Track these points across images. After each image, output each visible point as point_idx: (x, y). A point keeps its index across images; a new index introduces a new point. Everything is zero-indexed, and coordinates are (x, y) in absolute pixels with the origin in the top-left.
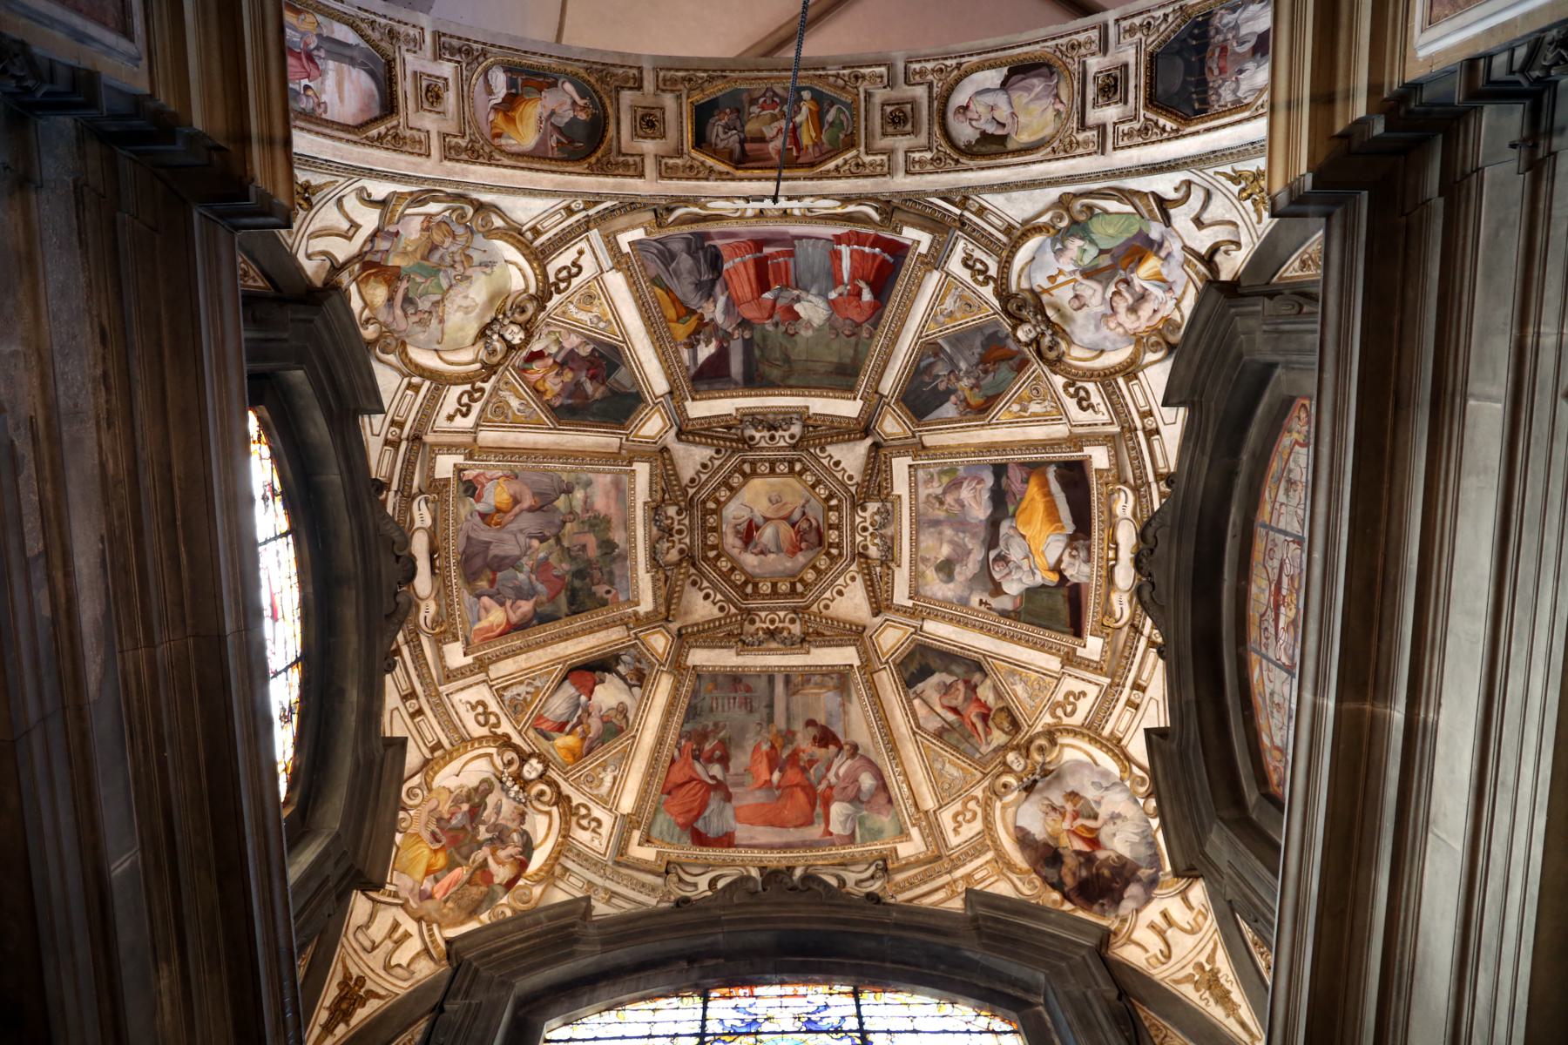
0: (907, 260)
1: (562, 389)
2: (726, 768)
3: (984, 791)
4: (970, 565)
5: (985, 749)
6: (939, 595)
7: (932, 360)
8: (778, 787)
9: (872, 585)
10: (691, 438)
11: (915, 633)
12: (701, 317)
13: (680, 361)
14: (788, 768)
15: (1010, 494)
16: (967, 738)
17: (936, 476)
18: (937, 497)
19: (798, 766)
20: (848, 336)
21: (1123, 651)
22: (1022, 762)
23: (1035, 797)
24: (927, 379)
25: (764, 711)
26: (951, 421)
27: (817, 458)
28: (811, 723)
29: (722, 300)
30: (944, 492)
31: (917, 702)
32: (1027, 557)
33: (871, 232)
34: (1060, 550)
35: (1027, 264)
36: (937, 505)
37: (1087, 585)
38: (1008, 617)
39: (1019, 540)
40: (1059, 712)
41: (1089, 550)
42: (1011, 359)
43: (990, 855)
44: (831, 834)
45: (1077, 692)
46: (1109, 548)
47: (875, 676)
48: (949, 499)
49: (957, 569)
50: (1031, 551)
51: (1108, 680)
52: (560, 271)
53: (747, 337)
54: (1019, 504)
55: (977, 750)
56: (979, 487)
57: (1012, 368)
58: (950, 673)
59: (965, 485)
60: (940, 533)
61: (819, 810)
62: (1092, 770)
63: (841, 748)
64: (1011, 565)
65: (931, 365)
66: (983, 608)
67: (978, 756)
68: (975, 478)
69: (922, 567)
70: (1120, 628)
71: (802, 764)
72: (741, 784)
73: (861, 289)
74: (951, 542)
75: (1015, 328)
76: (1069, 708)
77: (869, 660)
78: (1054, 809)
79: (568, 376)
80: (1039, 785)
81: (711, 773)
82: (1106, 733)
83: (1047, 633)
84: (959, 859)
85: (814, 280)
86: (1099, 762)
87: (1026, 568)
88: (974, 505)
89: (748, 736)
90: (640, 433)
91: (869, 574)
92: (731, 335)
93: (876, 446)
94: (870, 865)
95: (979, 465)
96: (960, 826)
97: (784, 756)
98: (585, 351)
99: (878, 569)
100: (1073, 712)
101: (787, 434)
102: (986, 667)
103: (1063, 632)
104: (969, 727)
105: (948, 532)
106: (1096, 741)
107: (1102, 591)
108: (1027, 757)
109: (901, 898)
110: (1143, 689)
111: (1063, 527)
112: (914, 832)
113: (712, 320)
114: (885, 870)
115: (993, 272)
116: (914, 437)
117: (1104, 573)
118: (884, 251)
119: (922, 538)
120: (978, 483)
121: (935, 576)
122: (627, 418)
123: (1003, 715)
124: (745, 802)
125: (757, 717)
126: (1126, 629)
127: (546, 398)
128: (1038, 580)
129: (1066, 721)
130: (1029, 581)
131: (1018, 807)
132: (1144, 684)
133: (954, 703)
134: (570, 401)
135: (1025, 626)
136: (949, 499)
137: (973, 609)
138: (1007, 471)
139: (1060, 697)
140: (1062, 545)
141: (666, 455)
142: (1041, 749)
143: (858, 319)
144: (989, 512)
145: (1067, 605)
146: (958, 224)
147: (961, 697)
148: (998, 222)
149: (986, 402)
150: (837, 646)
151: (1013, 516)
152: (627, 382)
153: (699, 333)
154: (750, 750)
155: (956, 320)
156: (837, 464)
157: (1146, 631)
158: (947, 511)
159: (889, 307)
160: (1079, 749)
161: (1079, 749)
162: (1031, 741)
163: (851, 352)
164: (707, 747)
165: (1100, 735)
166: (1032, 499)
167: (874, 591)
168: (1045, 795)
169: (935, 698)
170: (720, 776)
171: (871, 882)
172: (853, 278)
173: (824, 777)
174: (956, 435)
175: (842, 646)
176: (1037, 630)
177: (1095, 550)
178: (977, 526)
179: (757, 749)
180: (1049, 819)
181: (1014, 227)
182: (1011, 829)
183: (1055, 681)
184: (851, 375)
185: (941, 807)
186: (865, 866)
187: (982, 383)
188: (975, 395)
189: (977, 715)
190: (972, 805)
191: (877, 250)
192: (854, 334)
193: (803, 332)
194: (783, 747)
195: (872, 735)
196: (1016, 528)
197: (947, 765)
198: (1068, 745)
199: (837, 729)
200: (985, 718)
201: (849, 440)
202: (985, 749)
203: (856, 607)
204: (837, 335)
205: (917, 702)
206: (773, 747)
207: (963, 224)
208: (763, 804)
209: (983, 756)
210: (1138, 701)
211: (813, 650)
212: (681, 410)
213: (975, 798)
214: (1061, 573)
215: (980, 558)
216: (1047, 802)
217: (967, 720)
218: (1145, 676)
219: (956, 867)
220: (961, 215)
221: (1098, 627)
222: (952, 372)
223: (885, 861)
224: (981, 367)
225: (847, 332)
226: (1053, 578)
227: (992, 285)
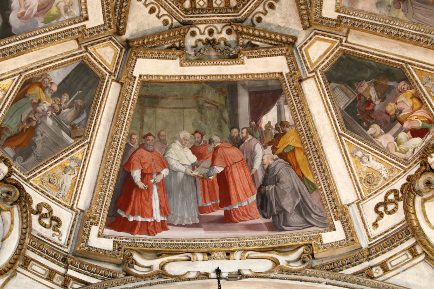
0: (106, 214)
1: (397, 96)
7: (77, 122)
10: (284, 39)
12: (274, 150)
13: (293, 110)
17: (63, 11)
20: (150, 134)
24: (79, 102)
26: (54, 67)
27: (171, 15)
29: (257, 166)
33: (137, 236)
35: (8, 236)
42: (9, 138)
52: (394, 211)
53: (235, 130)
56: (22, 10)
57: (7, 129)
59: (35, 10)
65: (77, 116)
68: (27, 18)
73: (142, 180)
75: (11, 172)
79: (391, 108)
85: (181, 185)
90: (329, 44)
92: (249, 132)
93: (119, 33)
95: (25, 31)
98: (375, 129)
101: (198, 36)
113: (265, 147)
115: (35, 218)
116: (86, 47)
118: (126, 219)
120: (23, 14)
122: (341, 59)
127: (413, 91)
134: (391, 84)
141: (307, 23)
143: (142, 152)
146: (69, 260)
148: (36, 268)
149: (26, 92)
152: (339, 94)
153: (276, 135)
155: (60, 165)
156: (152, 11)
159: (118, 167)
163: (146, 119)
172: (149, 190)
174: (49, 55)
181: (23, 266)
184: (145, 96)
187: (31, 108)
188: (36, 96)
191: (131, 219)
192: (145, 137)
193: (188, 135)
201: (143, 38)
204: (159, 135)
207: (64, 260)
212: (292, 63)
220: (67, 268)
222: (58, 114)
224: (34, 124)
225: (151, 138)
227: (34, 207)
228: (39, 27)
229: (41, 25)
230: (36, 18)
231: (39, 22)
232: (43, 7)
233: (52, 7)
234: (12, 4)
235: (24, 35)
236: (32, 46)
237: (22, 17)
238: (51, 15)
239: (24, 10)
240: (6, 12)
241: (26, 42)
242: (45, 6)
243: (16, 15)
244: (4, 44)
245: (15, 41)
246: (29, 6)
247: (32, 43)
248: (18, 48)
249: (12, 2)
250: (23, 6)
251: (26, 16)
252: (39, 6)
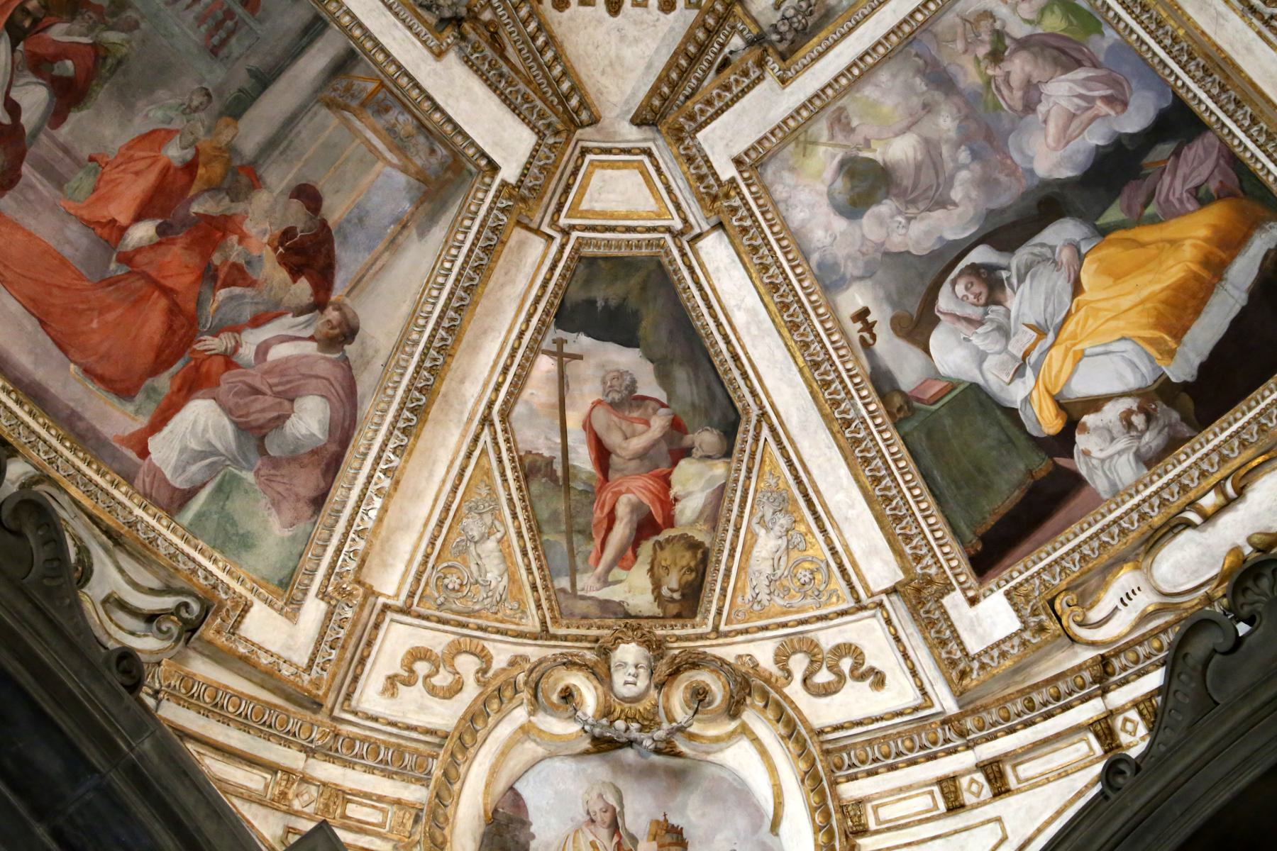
2: (56, 116)
3: (513, 663)
4: (917, 228)
5: (587, 583)
6: (797, 216)
8: (126, 259)
9: (693, 60)
11: (676, 235)
14: (182, 240)
15: (1146, 186)
16: (576, 530)
18: (999, 35)
19: (206, 256)
21: (1036, 687)
22: (642, 683)
23: (597, 769)
25: (242, 79)
28: (308, 196)
30: (1024, 44)
31: (545, 364)
32: (1041, 331)
34: (1118, 388)
36: (982, 51)
37: (1098, 501)
38: (883, 397)
39: (1062, 284)
40: (798, 664)
41: (1172, 445)
43: (415, 794)
44: (144, 453)
45: (870, 662)
46: (1219, 487)
47: (518, 234)
48: (1019, 66)
49: (885, 208)
50: (1059, 329)
51: (952, 707)
54: (1142, 221)
55: (573, 572)
56: (1102, 107)
58: (664, 377)
59: (1080, 74)
60: (928, 108)
61: (164, 383)
62: (756, 828)
63: (319, 304)
64: (995, 312)
66: (854, 329)
67: (564, 583)
68: (1112, 82)
69: (821, 128)
70: (1073, 640)
71: (216, 259)
72: (59, 181)
74: (930, 146)
76: (824, 676)
77: (537, 191)
78: (614, 827)
80: (629, 755)
81: (14, 95)
82: (850, 791)
83: (928, 502)
84: (352, 740)
86: (784, 828)
87: (1017, 346)
88: (1052, 128)
89: (161, 94)
91: (710, 33)
94: (167, 591)
95: (1151, 72)
96: (408, 683)
97: (196, 208)
99: (736, 42)
100: (826, 691)
102: (745, 436)
103: (955, 531)
104: (599, 515)
105: (946, 123)
106: (817, 787)
107: (1117, 545)
108: (660, 686)
109: (172, 712)
110: (1000, 789)
111: (1171, 354)
112: (313, 610)
114: (190, 629)
117: (1157, 518)
119: (883, 76)
120: (1108, 100)
121: (828, 174)
123: (686, 558)
124: (30, 223)
125: (215, 75)
126: (1087, 655)
128: (1016, 394)
129: (795, 690)
130: (994, 377)
131: (551, 756)
132: (1012, 783)
133: (613, 439)
135: (899, 447)
136: (1019, 66)
137: (833, 310)
138: (1190, 140)
139: (828, 637)
140: (1132, 382)
142: (699, 696)
144: (1066, 173)
145: (1017, 495)
147: (637, 443)
150: (505, 100)
151: (1103, 232)
154: (139, 126)
157: (1118, 697)
158: (989, 81)
160: (772, 769)
161: (772, 769)
162: (696, 662)
164: (59, 32)
165: (834, 783)
166: (1174, 243)
167: (684, 74)
168: (621, 784)
169: (586, 394)
170: (29, 119)
171: (137, 625)
173: (236, 329)
175: (515, 109)
176: (914, 475)
177: (1185, 460)
178: (1013, 171)
179: (156, 138)
180: (587, 836)
182: (501, 786)
183: (849, 603)
185: (405, 611)
186: (155, 583)
189: (636, 508)
190: (467, 665)
194: (213, 188)
195: (404, 342)
196: (1081, 258)
197: (491, 544)
198: (755, 740)
199: (348, 262)
200: (646, 527)
202: (587, 583)
203: (616, 66)
205: (545, 364)
206: (190, 168)
208: (63, 262)
209: (574, 594)
210: (968, 799)
211: (452, 58)
213: (484, 657)
214: (1071, 426)
215: (950, 236)
216: (612, 800)
217: (608, 496)
218: (1027, 770)
219: (330, 755)
221: (1039, 600)
223: (206, 611)
226: (1048, 422)
228: (1117, 37)
229: (1109, 32)
230: (1101, 58)
231: (1106, 44)
232: (1064, 58)
233: (1049, 31)
234: (1101, 143)
235: (1159, 68)
236: (1175, 40)
237: (1120, 97)
238: (1071, 23)
239: (1099, 103)
240: (1130, 148)
241: (1173, 58)
242: (1055, 53)
243: (1122, 116)
244: (1212, 113)
245: (1189, 90)
246: (1080, 96)
247: (1168, 42)
248: (1199, 74)
249: (1097, 147)
250: (1090, 114)
251: (1110, 87)
252: (1067, 69)
